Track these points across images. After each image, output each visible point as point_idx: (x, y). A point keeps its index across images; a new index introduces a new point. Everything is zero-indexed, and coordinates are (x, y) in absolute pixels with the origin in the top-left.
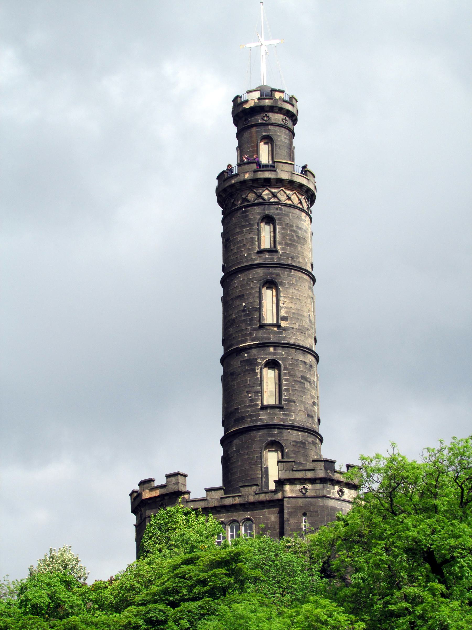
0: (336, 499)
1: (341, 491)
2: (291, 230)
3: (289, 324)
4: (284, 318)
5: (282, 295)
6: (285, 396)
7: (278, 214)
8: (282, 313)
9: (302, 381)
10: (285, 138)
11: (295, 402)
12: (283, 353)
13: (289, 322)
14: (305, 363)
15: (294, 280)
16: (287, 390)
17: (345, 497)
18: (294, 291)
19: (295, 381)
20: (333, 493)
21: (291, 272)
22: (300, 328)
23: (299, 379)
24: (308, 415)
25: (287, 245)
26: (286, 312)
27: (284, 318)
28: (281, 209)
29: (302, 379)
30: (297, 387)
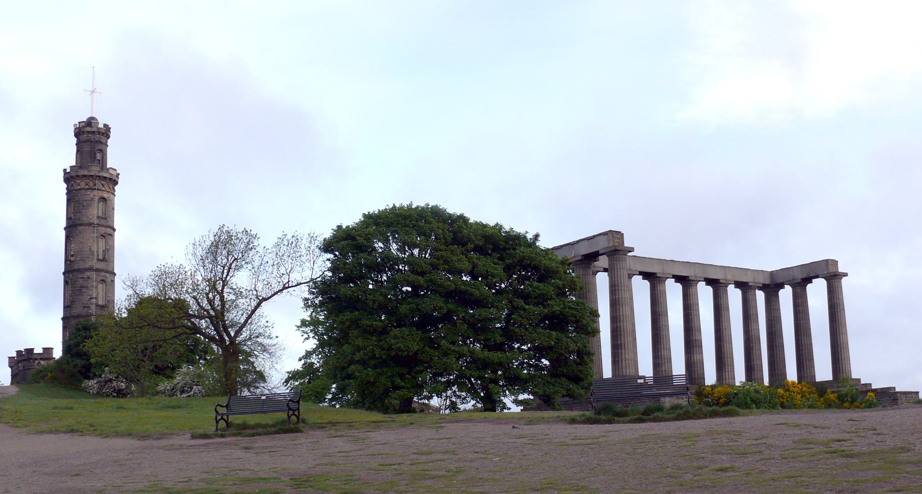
4: (72, 256)
27: (72, 256)
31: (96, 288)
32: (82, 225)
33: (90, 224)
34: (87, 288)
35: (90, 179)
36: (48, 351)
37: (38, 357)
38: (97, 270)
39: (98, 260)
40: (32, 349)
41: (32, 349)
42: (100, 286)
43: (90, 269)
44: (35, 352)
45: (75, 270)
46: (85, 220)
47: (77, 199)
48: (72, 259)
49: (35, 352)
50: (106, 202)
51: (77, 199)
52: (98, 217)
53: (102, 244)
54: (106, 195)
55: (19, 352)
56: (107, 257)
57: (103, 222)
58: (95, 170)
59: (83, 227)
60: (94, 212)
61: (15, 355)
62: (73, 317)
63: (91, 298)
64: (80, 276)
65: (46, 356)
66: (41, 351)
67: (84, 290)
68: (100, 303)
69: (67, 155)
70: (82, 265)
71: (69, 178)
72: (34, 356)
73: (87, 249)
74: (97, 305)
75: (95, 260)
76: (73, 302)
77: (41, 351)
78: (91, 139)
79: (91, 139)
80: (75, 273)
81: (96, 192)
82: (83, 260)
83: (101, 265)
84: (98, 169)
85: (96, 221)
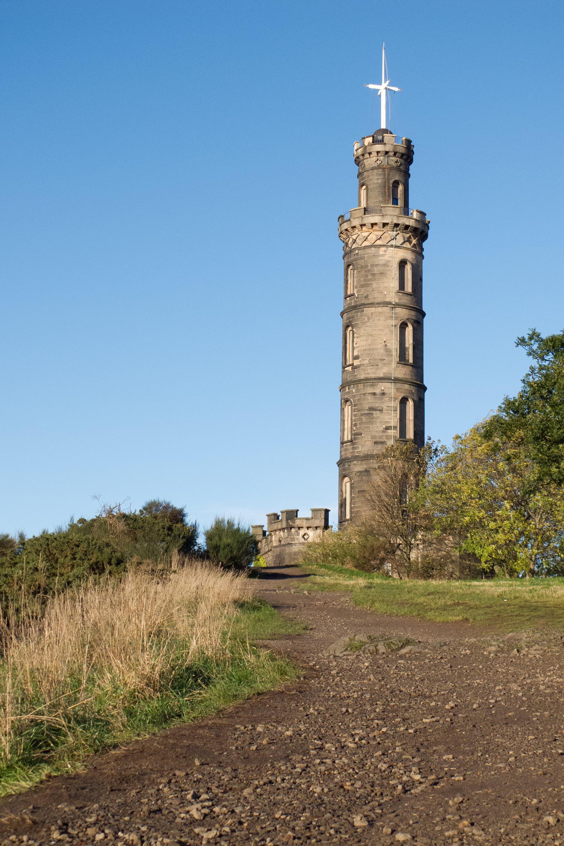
2: (365, 271)
3: (360, 361)
5: (355, 336)
6: (354, 431)
7: (356, 260)
8: (356, 353)
9: (371, 412)
10: (378, 179)
11: (361, 434)
12: (354, 390)
13: (360, 359)
14: (374, 394)
15: (366, 318)
18: (366, 328)
19: (362, 415)
20: (297, 539)
21: (363, 311)
22: (371, 361)
23: (366, 412)
24: (376, 443)
25: (362, 286)
26: (358, 351)
28: (357, 254)
29: (370, 411)
30: (364, 419)
32: (372, 304)
34: (381, 411)
45: (360, 381)
47: (361, 262)
48: (356, 363)
51: (361, 262)
59: (372, 310)
64: (370, 390)
66: (309, 515)
67: (376, 414)
72: (298, 523)
73: (381, 346)
75: (394, 365)
77: (309, 515)
80: (361, 386)
84: (397, 211)
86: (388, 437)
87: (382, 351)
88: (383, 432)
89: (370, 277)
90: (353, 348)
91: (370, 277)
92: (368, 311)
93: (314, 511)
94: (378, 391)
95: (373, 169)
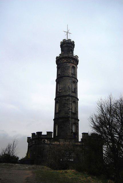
0: (43, 144)
1: (44, 140)
14: (65, 99)
16: (60, 108)
17: (46, 143)
31: (71, 104)
32: (65, 76)
33: (69, 76)
35: (67, 60)
36: (49, 133)
37: (44, 137)
38: (72, 96)
39: (72, 92)
40: (41, 133)
41: (41, 133)
42: (73, 104)
43: (69, 96)
44: (43, 134)
46: (67, 75)
49: (43, 134)
50: (75, 68)
52: (72, 74)
53: (73, 85)
54: (75, 66)
55: (33, 134)
56: (75, 91)
57: (74, 76)
58: (70, 55)
59: (65, 78)
60: (71, 71)
61: (31, 136)
62: (60, 118)
63: (69, 109)
65: (48, 137)
66: (46, 134)
68: (73, 112)
69: (58, 52)
70: (65, 94)
71: (59, 60)
74: (72, 113)
76: (60, 111)
77: (46, 134)
78: (67, 46)
79: (67, 46)
81: (70, 64)
82: (65, 91)
83: (73, 94)
85: (71, 76)
86: (70, 112)
87: (68, 88)
88: (68, 110)
89: (64, 70)
90: (60, 87)
91: (64, 70)
92: (64, 78)
93: (47, 132)
94: (66, 99)
95: (65, 46)
